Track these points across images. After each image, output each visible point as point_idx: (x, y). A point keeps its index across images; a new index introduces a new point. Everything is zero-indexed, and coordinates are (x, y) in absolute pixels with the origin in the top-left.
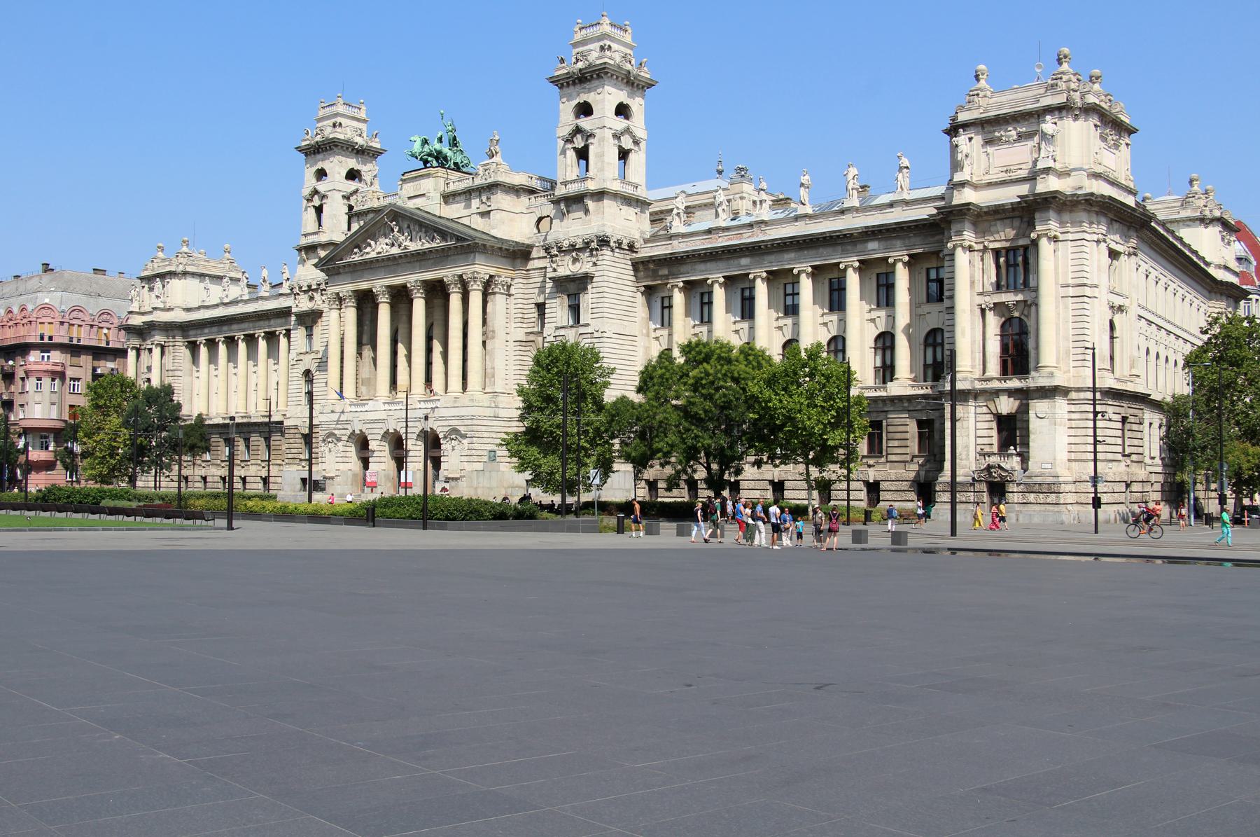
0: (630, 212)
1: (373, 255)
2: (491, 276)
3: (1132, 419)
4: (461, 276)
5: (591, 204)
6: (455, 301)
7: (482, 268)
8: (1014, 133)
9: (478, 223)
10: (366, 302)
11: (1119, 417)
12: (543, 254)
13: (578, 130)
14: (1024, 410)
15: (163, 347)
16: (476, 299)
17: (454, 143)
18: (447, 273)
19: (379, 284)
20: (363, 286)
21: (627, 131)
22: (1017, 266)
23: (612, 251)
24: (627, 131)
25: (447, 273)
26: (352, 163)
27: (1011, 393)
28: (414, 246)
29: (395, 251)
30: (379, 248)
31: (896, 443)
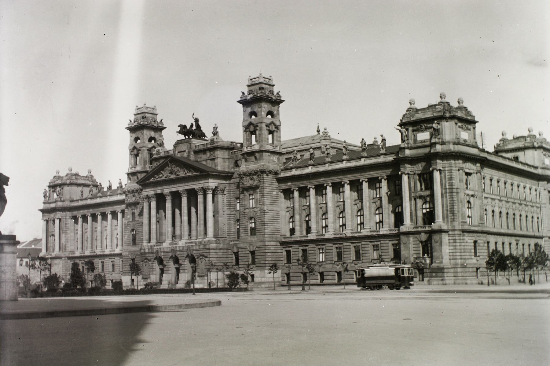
0: (275, 158)
1: (163, 178)
2: (216, 187)
3: (479, 241)
4: (202, 187)
5: (257, 155)
6: (200, 198)
7: (212, 183)
8: (424, 127)
9: (210, 164)
10: (161, 199)
11: (472, 241)
12: (237, 176)
13: (251, 124)
14: (430, 239)
15: (60, 220)
16: (210, 197)
17: (198, 127)
18: (196, 185)
19: (167, 190)
20: (159, 192)
21: (272, 123)
22: (427, 179)
23: (267, 175)
24: (272, 123)
25: (196, 185)
26: (152, 134)
27: (426, 232)
28: (182, 174)
29: (173, 176)
30: (165, 175)
31: (385, 254)
